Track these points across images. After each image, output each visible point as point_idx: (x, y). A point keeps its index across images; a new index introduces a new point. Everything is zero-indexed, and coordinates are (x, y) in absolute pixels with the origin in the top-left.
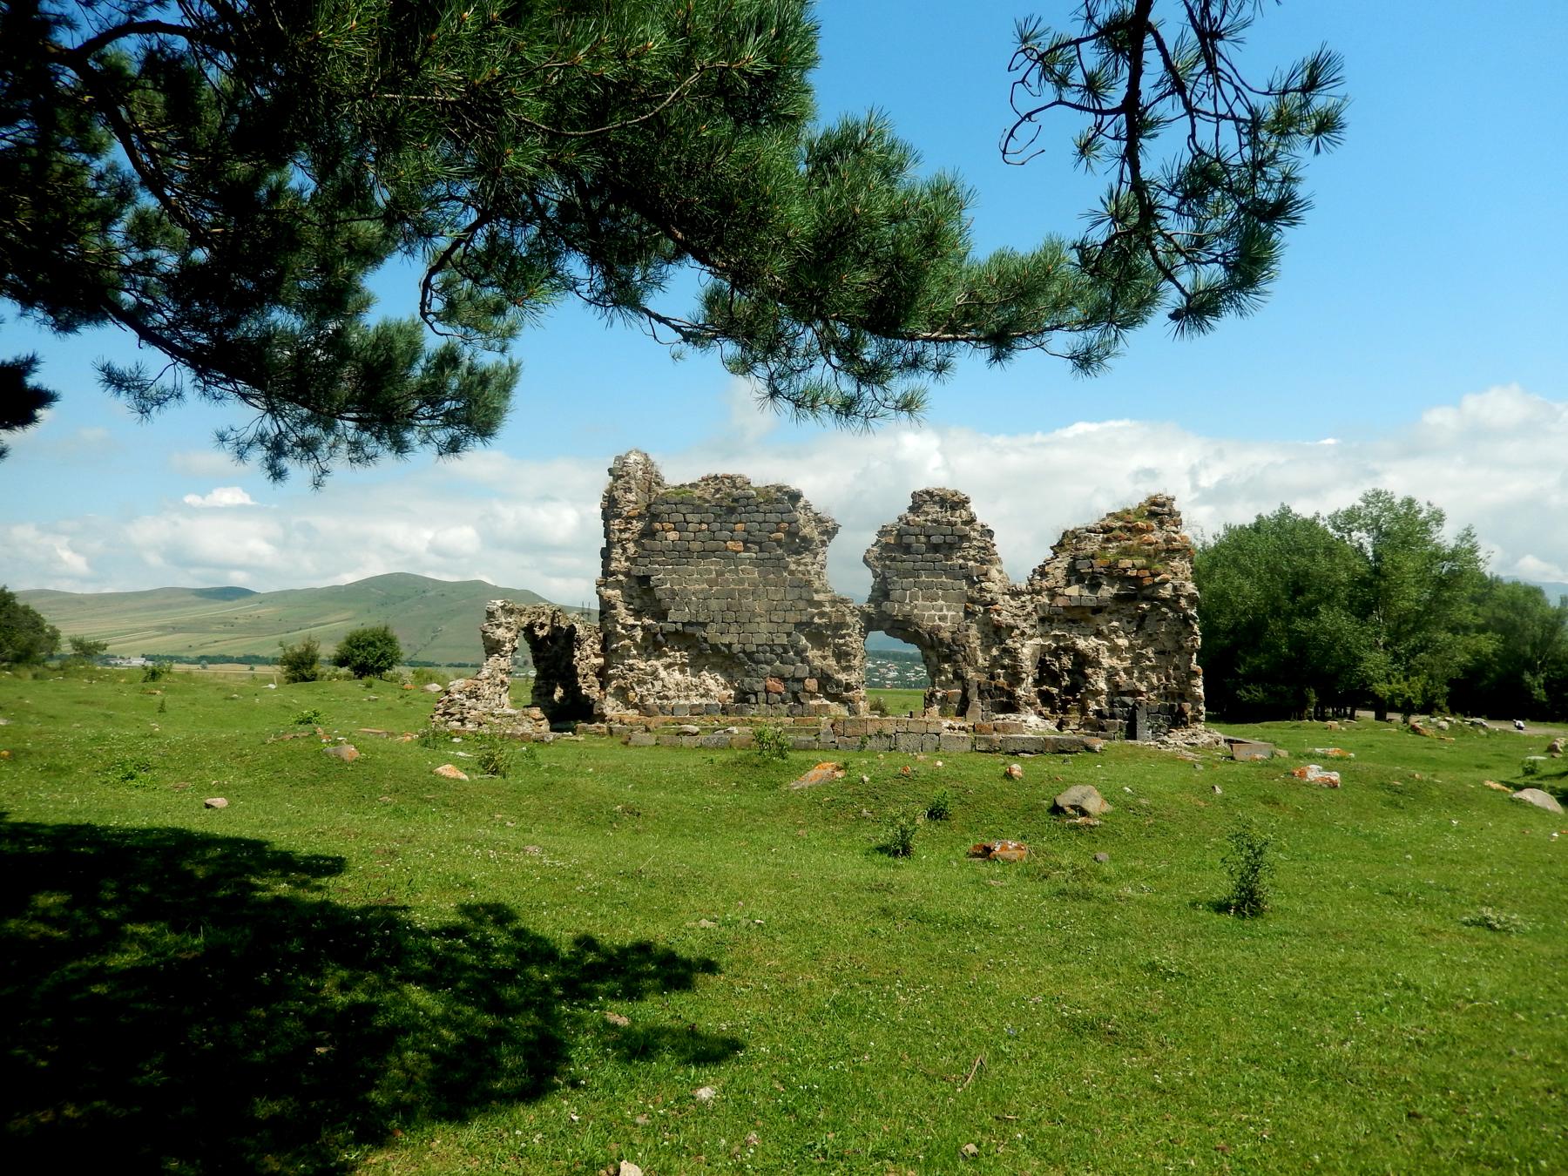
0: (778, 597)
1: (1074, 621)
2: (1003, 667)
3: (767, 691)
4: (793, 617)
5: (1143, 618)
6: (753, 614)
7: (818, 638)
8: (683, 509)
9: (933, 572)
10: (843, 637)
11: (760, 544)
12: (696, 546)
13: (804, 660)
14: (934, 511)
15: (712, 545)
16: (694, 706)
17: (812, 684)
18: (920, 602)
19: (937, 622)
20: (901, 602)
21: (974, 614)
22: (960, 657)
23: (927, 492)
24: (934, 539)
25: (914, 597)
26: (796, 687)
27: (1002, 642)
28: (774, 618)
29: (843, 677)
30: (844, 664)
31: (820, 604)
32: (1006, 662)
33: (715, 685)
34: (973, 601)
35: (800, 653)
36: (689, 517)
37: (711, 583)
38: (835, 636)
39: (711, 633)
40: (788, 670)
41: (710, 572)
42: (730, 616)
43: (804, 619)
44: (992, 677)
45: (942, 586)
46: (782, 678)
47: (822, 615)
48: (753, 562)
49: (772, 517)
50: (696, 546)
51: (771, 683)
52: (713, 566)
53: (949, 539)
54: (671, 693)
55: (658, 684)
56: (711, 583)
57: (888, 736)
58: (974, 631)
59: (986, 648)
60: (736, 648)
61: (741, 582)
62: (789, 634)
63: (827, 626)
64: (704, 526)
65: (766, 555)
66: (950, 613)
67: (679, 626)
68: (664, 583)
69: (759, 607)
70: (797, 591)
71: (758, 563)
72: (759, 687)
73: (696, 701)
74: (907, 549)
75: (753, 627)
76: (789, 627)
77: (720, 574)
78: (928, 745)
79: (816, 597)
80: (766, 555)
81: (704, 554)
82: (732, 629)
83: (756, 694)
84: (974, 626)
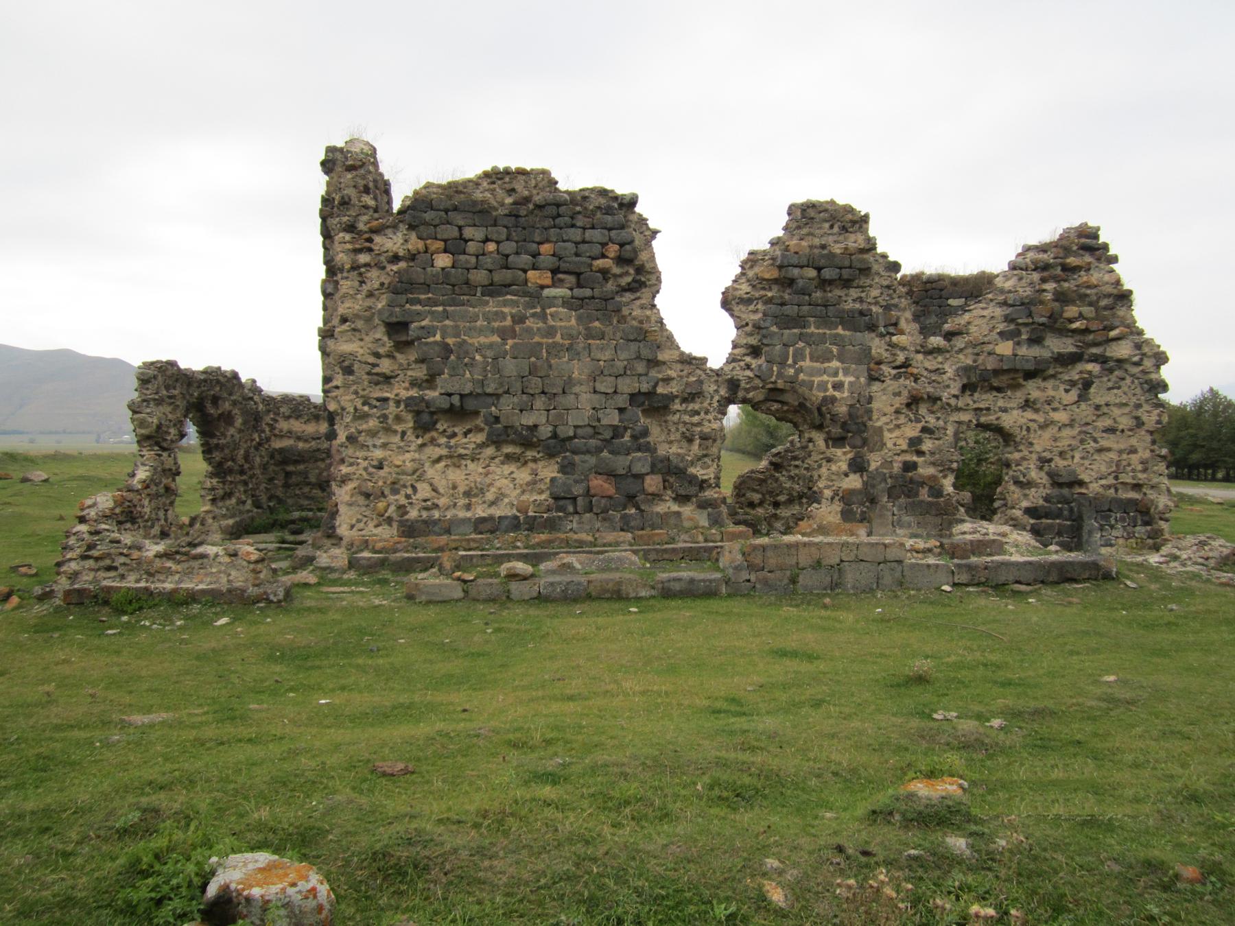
0: (608, 355)
3: (588, 493)
4: (627, 386)
5: (1087, 385)
6: (570, 382)
8: (459, 219)
9: (824, 321)
11: (578, 275)
12: (479, 276)
15: (507, 275)
16: (483, 520)
18: (806, 363)
19: (831, 392)
20: (783, 364)
24: (828, 273)
25: (799, 356)
28: (601, 387)
33: (513, 485)
36: (468, 232)
37: (504, 334)
39: (507, 407)
40: (620, 463)
41: (501, 316)
42: (535, 383)
43: (645, 387)
45: (837, 340)
46: (611, 474)
48: (566, 303)
49: (596, 235)
50: (479, 276)
51: (599, 484)
52: (506, 308)
53: (846, 273)
54: (442, 501)
55: (424, 491)
56: (504, 334)
60: (545, 431)
61: (551, 332)
62: (621, 410)
64: (491, 247)
65: (587, 292)
67: (456, 400)
68: (430, 331)
69: (578, 370)
70: (634, 346)
71: (572, 304)
72: (578, 490)
73: (480, 512)
74: (791, 282)
75: (569, 400)
76: (622, 401)
77: (519, 319)
78: (887, 580)
80: (587, 292)
81: (493, 290)
82: (539, 403)
83: (574, 499)
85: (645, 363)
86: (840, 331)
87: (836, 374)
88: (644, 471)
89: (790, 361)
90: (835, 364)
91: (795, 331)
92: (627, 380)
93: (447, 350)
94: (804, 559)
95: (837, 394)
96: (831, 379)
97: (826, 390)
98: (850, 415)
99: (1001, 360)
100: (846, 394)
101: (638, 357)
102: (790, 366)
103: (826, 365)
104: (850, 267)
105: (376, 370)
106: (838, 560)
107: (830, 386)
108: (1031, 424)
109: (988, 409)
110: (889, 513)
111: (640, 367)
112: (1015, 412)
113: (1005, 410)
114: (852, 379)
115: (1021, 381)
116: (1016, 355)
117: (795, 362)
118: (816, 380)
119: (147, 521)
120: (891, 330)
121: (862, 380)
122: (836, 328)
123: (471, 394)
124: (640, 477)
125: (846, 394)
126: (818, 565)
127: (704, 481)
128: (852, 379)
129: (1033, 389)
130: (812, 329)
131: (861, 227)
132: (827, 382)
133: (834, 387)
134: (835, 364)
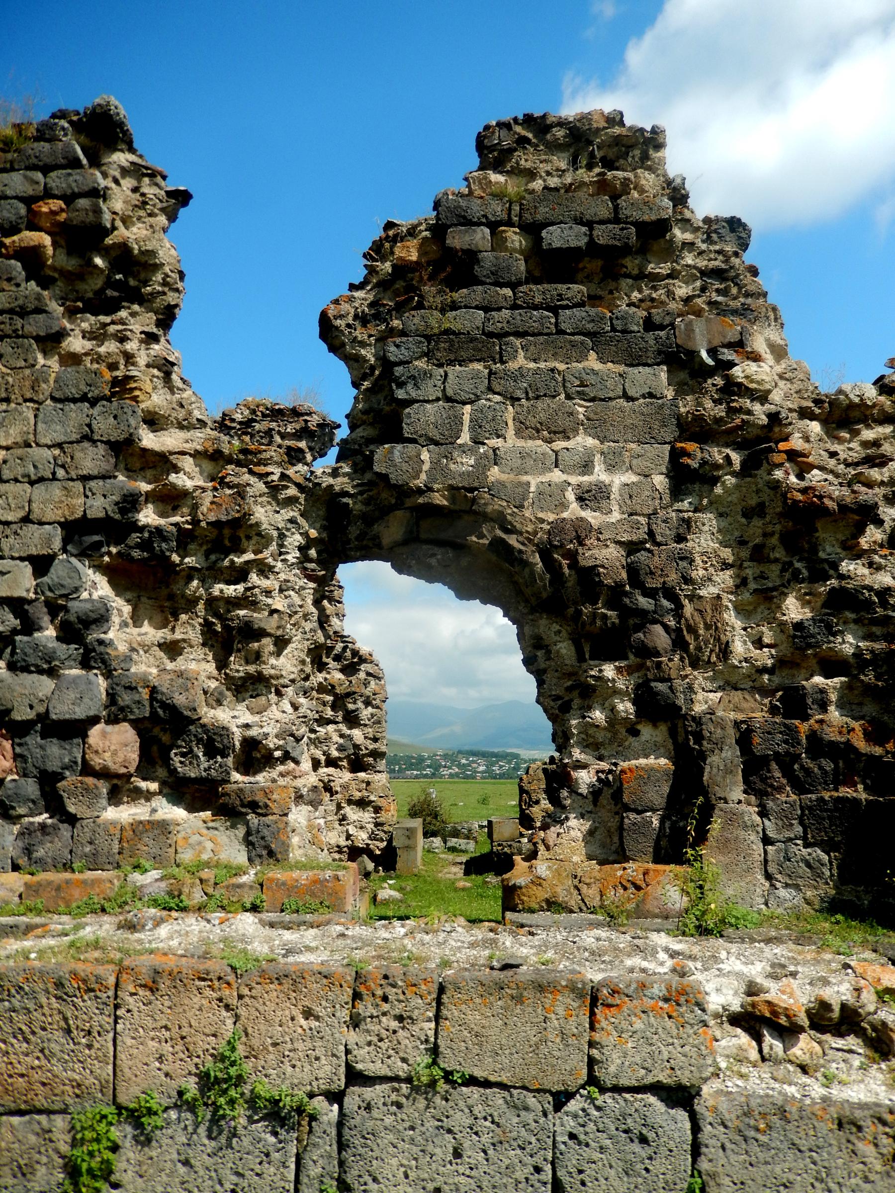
2: (832, 666)
7: (151, 581)
10: (239, 575)
13: (93, 658)
14: (552, 170)
17: (116, 745)
18: (510, 442)
19: (573, 511)
20: (443, 442)
21: (706, 477)
22: (659, 637)
23: (529, 120)
24: (556, 237)
26: (56, 754)
27: (821, 570)
29: (234, 718)
30: (238, 667)
31: (162, 463)
32: (848, 644)
34: (696, 430)
35: (80, 630)
38: (212, 573)
43: (99, 506)
44: (794, 704)
47: (170, 499)
53: (603, 235)
57: (276, 1115)
58: (706, 540)
59: (761, 600)
62: (41, 565)
63: (184, 539)
66: (618, 480)
70: (77, 414)
79: (149, 440)
84: (708, 521)
85: (101, 449)
86: (592, 362)
87: (586, 467)
88: (80, 713)
89: (465, 438)
90: (584, 441)
91: (478, 366)
92: (56, 491)
94: (149, 1059)
95: (592, 517)
96: (574, 479)
97: (563, 505)
98: (633, 571)
100: (616, 516)
101: (88, 437)
102: (463, 449)
103: (559, 445)
106: (329, 1072)
107: (571, 496)
110: (754, 838)
111: (91, 459)
114: (631, 478)
117: (478, 442)
118: (534, 481)
120: (728, 355)
121: (660, 481)
122: (583, 357)
124: (76, 730)
125: (616, 516)
126: (215, 1093)
128: (631, 478)
130: (521, 361)
131: (645, 157)
133: (580, 499)
134: (584, 441)
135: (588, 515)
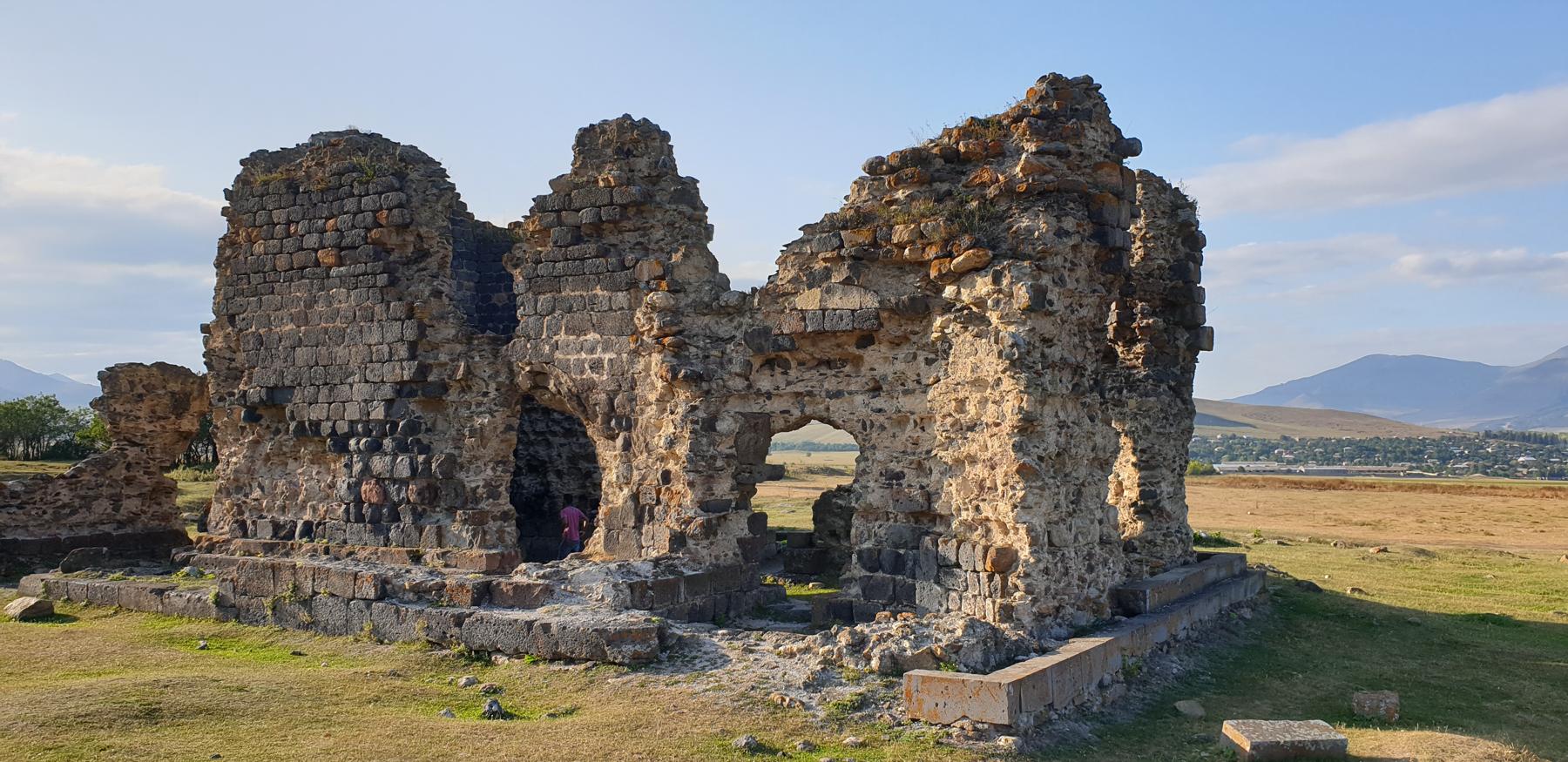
1: (828, 363)
18: (562, 337)
19: (588, 374)
76: (387, 391)
93: (260, 341)
99: (804, 319)
104: (611, 204)
105: (233, 365)
108: (874, 417)
109: (810, 394)
112: (859, 399)
113: (838, 394)
115: (853, 350)
116: (824, 310)
119: (64, 506)
123: (276, 387)
127: (474, 490)
129: (876, 359)
132: (583, 361)
135: (595, 376)
